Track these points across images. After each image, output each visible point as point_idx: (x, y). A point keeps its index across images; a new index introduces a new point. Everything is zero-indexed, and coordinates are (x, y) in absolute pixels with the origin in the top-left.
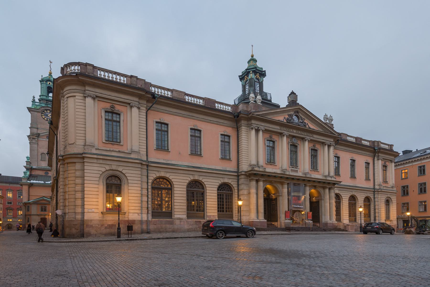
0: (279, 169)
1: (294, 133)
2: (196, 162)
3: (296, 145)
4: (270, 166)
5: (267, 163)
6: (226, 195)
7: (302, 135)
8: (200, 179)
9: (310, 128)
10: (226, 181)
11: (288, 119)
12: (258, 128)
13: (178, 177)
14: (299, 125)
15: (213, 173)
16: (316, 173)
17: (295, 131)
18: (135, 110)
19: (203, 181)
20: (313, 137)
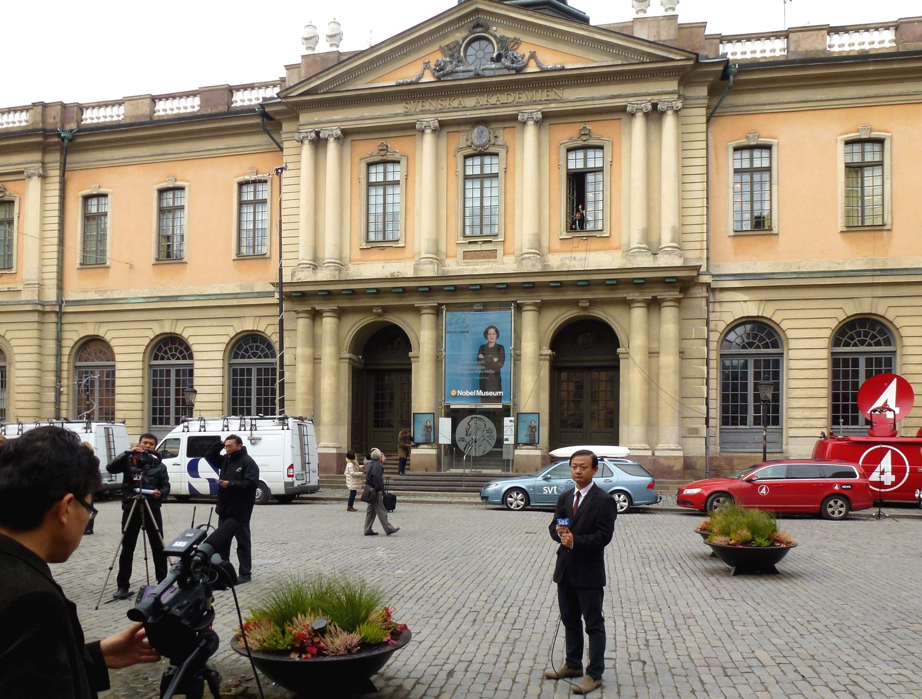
0: (413, 258)
1: (470, 106)
2: (174, 283)
3: (492, 150)
4: (376, 254)
5: (364, 246)
6: (259, 370)
7: (505, 105)
8: (178, 331)
9: (543, 71)
10: (249, 325)
11: (440, 68)
12: (318, 133)
13: (124, 333)
14: (478, 76)
15: (209, 307)
16: (594, 244)
17: (470, 102)
18: (34, 184)
19: (185, 335)
20: (561, 101)
